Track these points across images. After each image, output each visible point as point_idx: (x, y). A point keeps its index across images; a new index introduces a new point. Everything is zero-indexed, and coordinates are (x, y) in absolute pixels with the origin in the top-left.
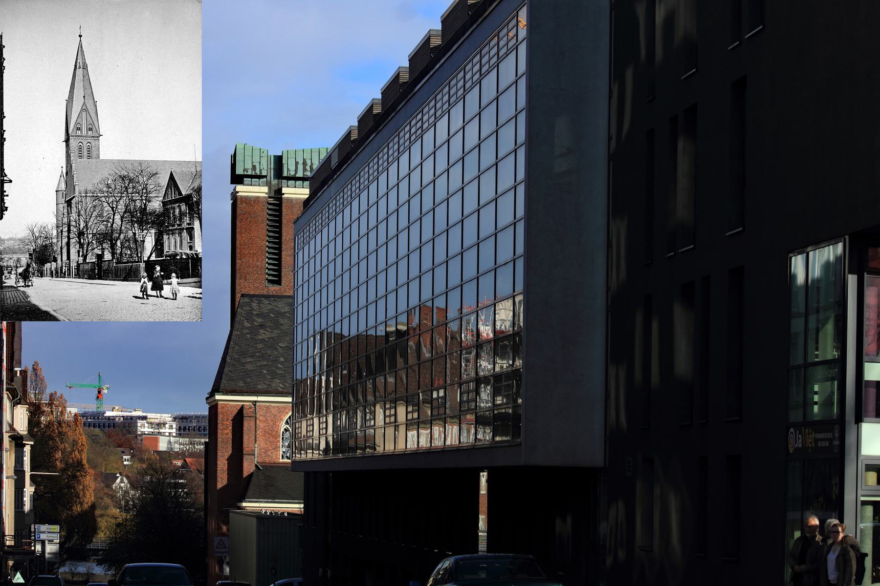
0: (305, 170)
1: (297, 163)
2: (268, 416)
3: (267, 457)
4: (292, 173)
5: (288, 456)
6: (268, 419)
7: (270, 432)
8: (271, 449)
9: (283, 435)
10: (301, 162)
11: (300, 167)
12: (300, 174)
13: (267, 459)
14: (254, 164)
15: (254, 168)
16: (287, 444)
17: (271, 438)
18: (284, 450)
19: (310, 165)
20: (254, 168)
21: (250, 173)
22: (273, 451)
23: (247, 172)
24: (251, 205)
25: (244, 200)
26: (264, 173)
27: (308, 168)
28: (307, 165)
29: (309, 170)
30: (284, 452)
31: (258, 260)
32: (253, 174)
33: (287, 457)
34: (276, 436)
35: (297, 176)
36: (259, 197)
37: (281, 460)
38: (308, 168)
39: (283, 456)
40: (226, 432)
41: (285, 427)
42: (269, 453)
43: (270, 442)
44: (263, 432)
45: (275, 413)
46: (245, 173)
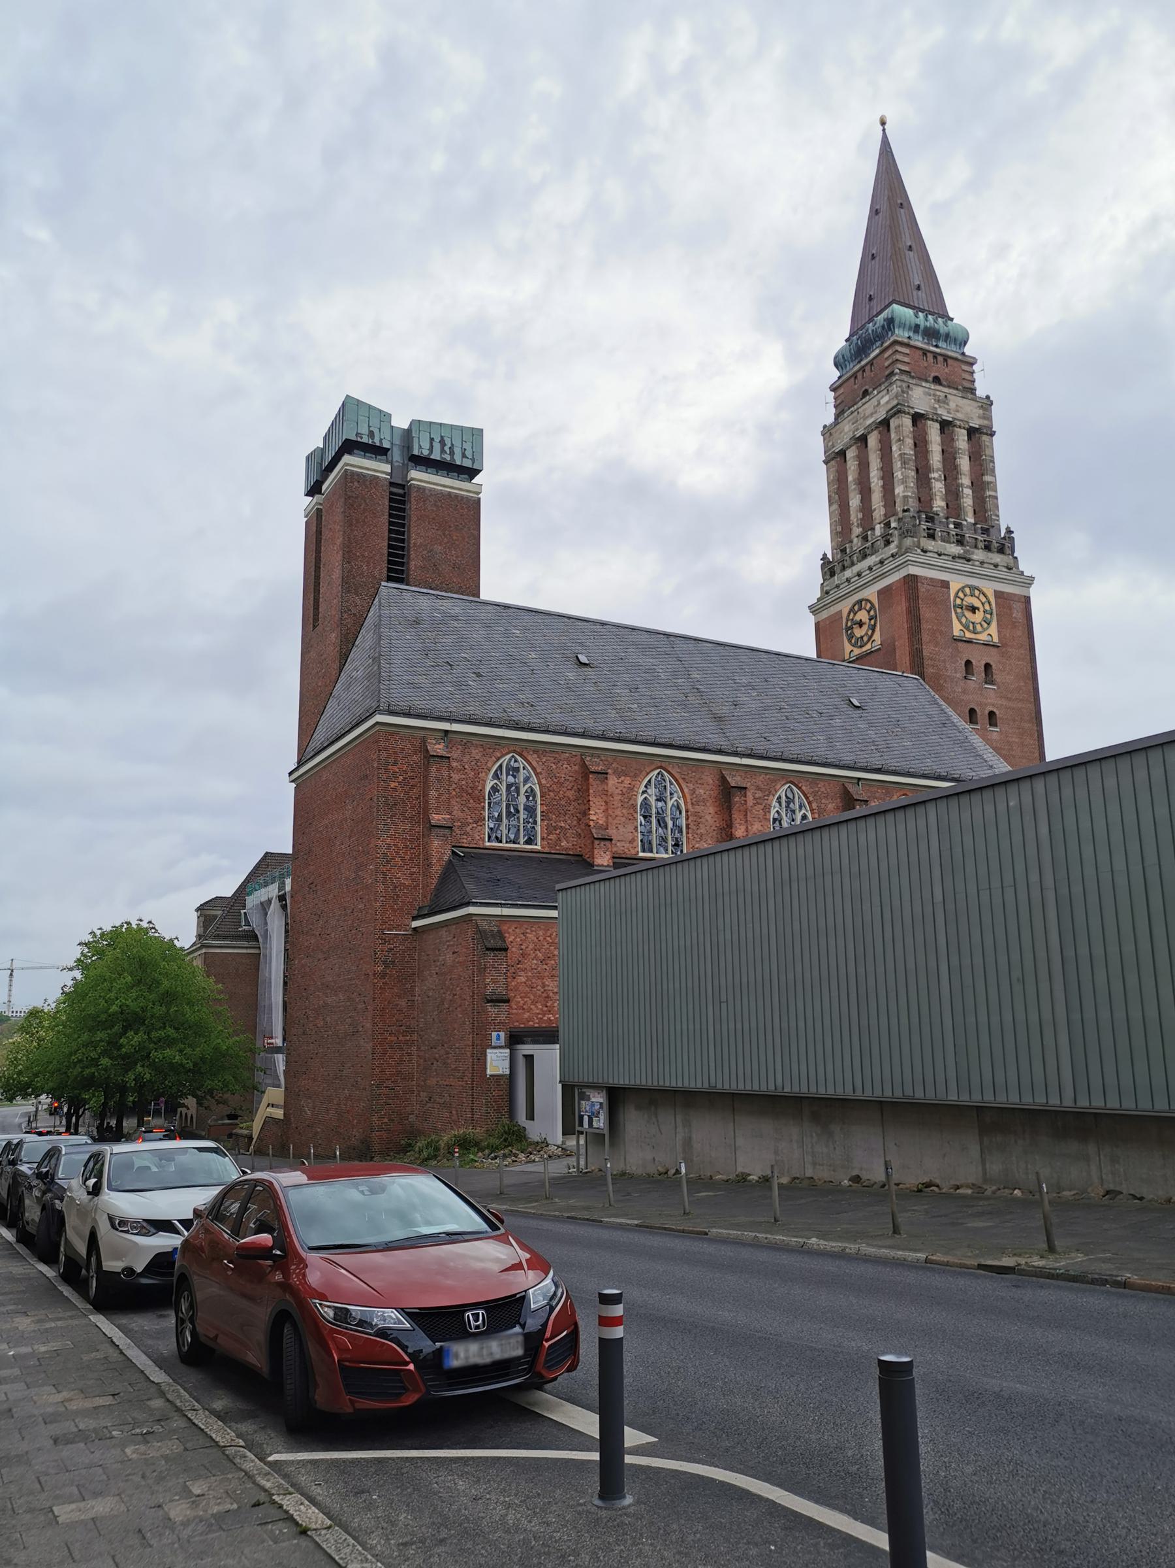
0: (443, 451)
1: (432, 440)
2: (465, 760)
3: (465, 837)
4: (426, 453)
5: (499, 836)
6: (466, 767)
7: (470, 791)
8: (471, 821)
9: (489, 799)
10: (437, 439)
11: (437, 446)
12: (436, 456)
13: (465, 841)
14: (371, 429)
15: (371, 434)
16: (496, 814)
17: (471, 801)
18: (492, 825)
19: (449, 445)
20: (371, 434)
21: (365, 440)
22: (475, 825)
23: (362, 438)
24: (367, 487)
25: (356, 477)
26: (386, 445)
27: (447, 449)
28: (445, 445)
29: (448, 452)
30: (491, 829)
31: (375, 568)
32: (370, 443)
33: (497, 837)
34: (479, 799)
35: (431, 457)
36: (378, 477)
37: (488, 844)
38: (447, 449)
39: (489, 837)
40: (393, 785)
41: (492, 783)
42: (468, 829)
43: (469, 808)
44: (457, 790)
45: (477, 758)
46: (359, 439)
